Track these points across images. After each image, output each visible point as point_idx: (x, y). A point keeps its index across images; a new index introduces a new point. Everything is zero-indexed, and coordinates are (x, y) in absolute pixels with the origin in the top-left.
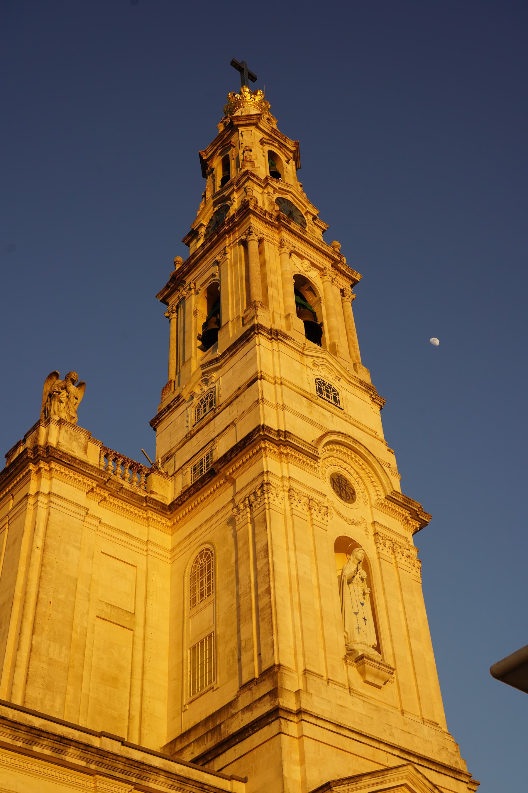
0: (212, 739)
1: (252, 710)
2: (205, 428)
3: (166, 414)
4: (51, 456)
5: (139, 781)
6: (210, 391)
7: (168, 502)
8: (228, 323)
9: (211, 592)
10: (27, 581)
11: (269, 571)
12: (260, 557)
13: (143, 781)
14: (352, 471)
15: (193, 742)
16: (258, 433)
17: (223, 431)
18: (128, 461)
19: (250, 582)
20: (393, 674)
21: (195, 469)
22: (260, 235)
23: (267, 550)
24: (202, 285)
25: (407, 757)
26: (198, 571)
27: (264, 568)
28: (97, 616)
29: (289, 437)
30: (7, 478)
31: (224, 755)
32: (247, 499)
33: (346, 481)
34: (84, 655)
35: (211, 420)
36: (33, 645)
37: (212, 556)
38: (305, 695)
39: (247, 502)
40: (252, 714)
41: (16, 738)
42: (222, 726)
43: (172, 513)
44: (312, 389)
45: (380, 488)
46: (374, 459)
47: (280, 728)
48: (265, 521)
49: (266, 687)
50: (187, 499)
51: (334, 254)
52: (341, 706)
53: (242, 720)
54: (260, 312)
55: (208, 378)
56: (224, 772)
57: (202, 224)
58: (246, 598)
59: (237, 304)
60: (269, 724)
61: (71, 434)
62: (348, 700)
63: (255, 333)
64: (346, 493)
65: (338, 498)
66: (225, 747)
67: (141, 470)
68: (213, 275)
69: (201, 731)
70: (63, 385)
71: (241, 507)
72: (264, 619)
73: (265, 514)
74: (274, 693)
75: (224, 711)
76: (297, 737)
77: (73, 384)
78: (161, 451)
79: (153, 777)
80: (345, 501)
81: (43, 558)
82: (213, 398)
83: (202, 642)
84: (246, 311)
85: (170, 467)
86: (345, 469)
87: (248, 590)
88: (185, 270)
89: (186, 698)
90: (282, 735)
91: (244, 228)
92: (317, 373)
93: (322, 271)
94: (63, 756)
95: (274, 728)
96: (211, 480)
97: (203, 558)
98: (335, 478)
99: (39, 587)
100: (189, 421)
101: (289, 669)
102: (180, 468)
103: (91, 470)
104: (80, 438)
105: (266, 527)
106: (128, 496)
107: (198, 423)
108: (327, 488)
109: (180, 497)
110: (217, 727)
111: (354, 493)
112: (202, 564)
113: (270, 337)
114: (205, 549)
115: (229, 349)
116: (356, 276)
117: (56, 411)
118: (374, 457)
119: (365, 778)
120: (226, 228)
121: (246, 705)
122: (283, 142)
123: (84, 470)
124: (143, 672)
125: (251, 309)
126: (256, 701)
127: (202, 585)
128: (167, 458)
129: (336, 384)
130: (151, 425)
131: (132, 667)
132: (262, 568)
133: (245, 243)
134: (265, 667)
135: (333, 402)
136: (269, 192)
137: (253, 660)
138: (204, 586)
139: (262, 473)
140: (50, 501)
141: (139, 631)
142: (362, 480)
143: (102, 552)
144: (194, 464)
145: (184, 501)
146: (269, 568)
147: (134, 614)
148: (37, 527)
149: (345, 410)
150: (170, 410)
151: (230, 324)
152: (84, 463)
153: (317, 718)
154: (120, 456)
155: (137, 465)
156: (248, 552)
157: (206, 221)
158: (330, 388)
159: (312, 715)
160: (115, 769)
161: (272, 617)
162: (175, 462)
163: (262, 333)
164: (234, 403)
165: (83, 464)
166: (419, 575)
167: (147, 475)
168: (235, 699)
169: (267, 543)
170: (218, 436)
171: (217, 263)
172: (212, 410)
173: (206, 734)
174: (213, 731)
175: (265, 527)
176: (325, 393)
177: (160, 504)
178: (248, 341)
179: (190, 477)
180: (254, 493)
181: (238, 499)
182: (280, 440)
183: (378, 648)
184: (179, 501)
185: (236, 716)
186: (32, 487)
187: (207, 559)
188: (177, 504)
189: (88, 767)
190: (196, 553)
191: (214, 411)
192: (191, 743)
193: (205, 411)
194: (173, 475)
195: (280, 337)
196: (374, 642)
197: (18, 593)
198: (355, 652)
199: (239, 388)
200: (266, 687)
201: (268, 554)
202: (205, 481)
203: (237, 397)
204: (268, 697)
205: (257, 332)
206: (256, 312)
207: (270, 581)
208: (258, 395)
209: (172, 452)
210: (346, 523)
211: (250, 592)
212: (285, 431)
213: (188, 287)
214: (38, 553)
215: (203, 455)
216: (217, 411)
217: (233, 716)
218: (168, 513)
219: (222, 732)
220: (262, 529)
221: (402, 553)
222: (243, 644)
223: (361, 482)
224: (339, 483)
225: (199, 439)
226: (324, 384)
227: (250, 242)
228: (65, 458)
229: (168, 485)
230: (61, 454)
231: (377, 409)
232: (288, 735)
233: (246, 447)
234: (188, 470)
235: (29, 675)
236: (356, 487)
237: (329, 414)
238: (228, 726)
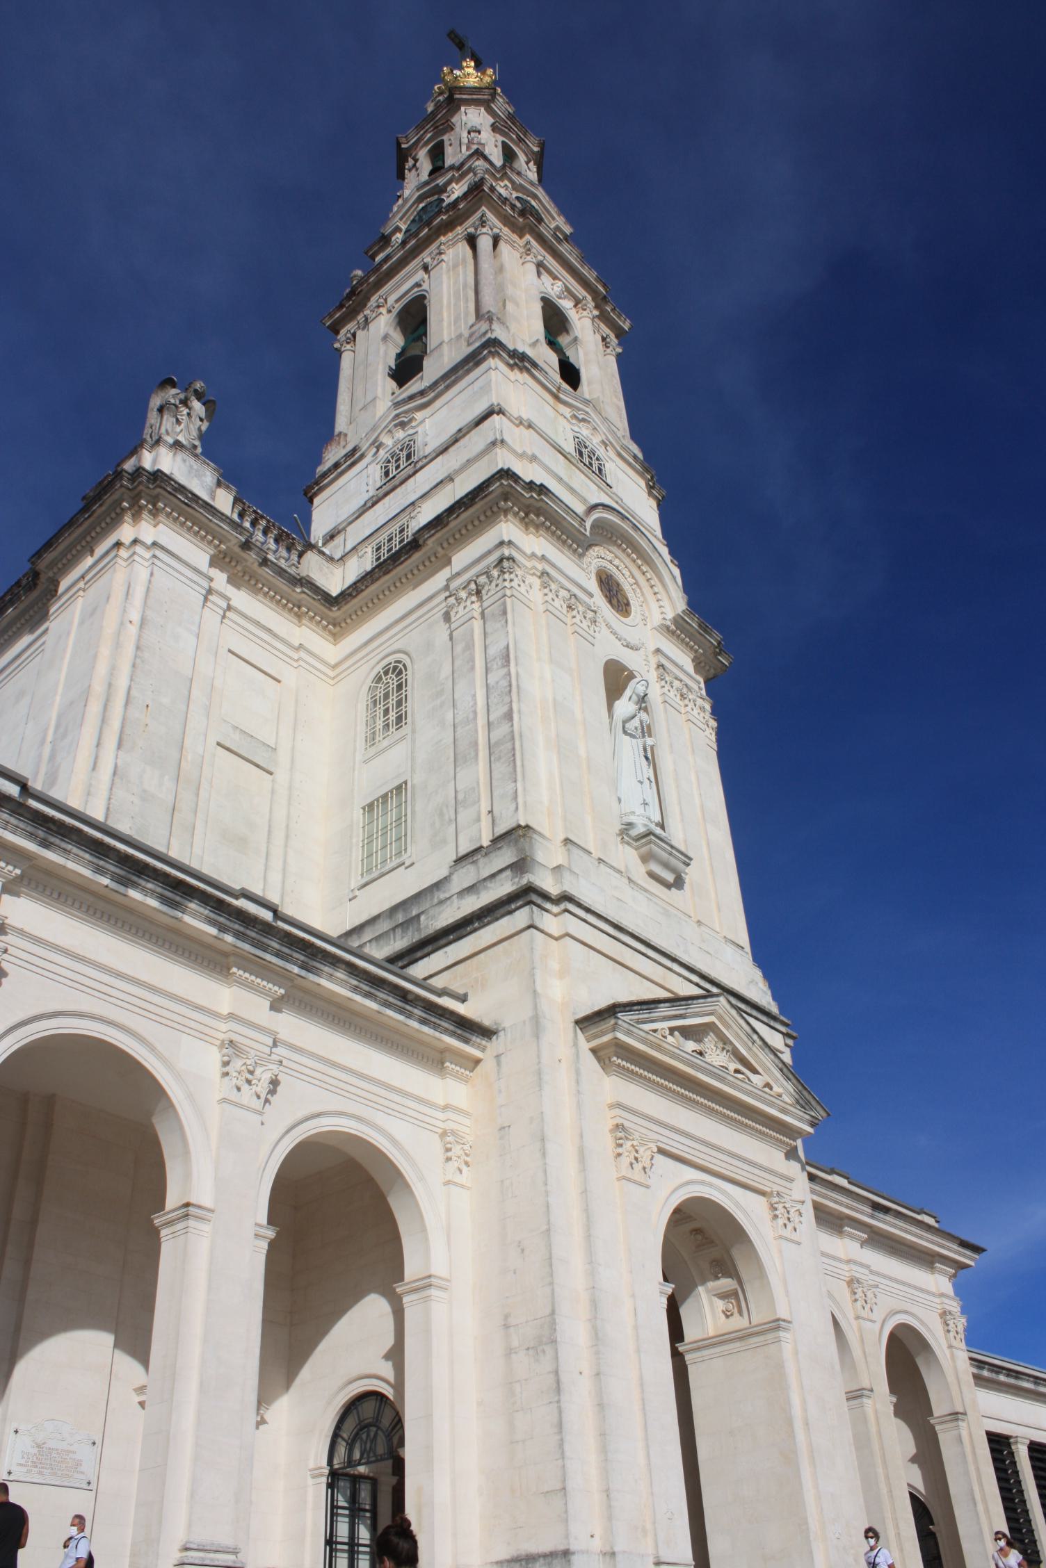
0: (402, 937)
1: (478, 893)
2: (399, 490)
3: (332, 476)
4: (161, 487)
5: (303, 973)
6: (407, 439)
7: (334, 594)
8: (441, 344)
9: (403, 723)
10: (113, 670)
11: (510, 685)
12: (495, 667)
13: (310, 974)
14: (625, 572)
15: (370, 941)
16: (499, 481)
17: (431, 489)
18: (274, 526)
19: (475, 704)
20: (688, 865)
21: (378, 549)
22: (496, 231)
23: (508, 656)
24: (397, 301)
25: (708, 986)
26: (380, 693)
27: (501, 683)
28: (219, 744)
29: (546, 495)
30: (86, 519)
31: (426, 960)
32: (473, 583)
33: (618, 585)
34: (198, 795)
35: (410, 477)
36: (119, 764)
37: (406, 670)
38: (568, 873)
39: (473, 586)
40: (478, 898)
41: (99, 870)
42: (423, 918)
43: (339, 609)
44: (570, 448)
45: (666, 602)
46: (660, 559)
47: (532, 918)
48: (505, 613)
49: (506, 856)
50: (367, 587)
51: (597, 282)
52: (619, 899)
53: (459, 908)
54: (495, 326)
55: (406, 420)
56: (432, 982)
57: (398, 229)
58: (467, 728)
59: (457, 319)
60: (510, 912)
61: (191, 467)
62: (628, 893)
63: (490, 352)
64: (618, 601)
65: (607, 604)
66: (429, 948)
67: (293, 544)
68: (418, 285)
69: (384, 926)
70: (182, 396)
71: (463, 594)
72: (500, 758)
73: (504, 604)
74: (520, 866)
75: (426, 895)
76: (556, 934)
77: (199, 399)
78: (318, 531)
79: (326, 969)
80: (617, 612)
81: (140, 637)
82: (412, 449)
83: (385, 797)
84: (472, 326)
85: (336, 547)
86: (617, 568)
87: (471, 716)
88: (371, 280)
89: (356, 881)
90: (532, 930)
91: (474, 218)
92: (576, 429)
93: (577, 302)
94: (180, 914)
95: (521, 917)
96: (410, 557)
97: (390, 675)
98: (604, 577)
99: (131, 680)
100: (371, 483)
101: (540, 834)
102: (354, 548)
103: (222, 520)
104: (205, 475)
105: (506, 621)
106: (273, 572)
107: (385, 484)
108: (593, 585)
109: (355, 583)
110: (412, 919)
111: (628, 604)
112: (388, 683)
113: (511, 362)
114: (393, 661)
115: (445, 377)
116: (624, 323)
117: (170, 430)
118: (660, 555)
119: (662, 1005)
120: (444, 218)
121: (466, 885)
122: (522, 136)
123: (210, 518)
124: (287, 837)
125: (482, 322)
126: (485, 880)
127: (386, 712)
128: (331, 537)
129: (601, 451)
130: (305, 494)
131: (270, 826)
132: (497, 683)
133: (472, 241)
134: (500, 830)
135: (597, 472)
136: (506, 185)
137: (478, 820)
138: (390, 716)
139: (502, 543)
140: (154, 556)
141: (282, 775)
142: (640, 589)
143: (230, 651)
144: (377, 541)
145: (362, 591)
146: (510, 682)
147: (275, 749)
148: (131, 591)
149: (614, 490)
150: (339, 470)
151: (445, 348)
152: (211, 506)
153: (588, 910)
154: (262, 517)
155: (288, 535)
156: (472, 660)
157: (405, 223)
158: (594, 455)
159: (579, 905)
160: (265, 948)
161: (514, 755)
162: (345, 540)
163: (501, 353)
164: (451, 450)
165: (208, 507)
166: (713, 738)
167: (300, 556)
168: (445, 878)
169: (507, 647)
170: (421, 497)
171: (426, 268)
172: (410, 464)
173: (394, 929)
174: (404, 925)
175: (503, 622)
176: (588, 459)
177: (322, 593)
178: (478, 364)
179: (371, 560)
180: (487, 573)
181: (454, 585)
182: (532, 496)
183: (662, 827)
184: (354, 589)
185: (448, 902)
186: (126, 532)
187: (396, 676)
188: (350, 595)
189: (220, 937)
190: (379, 668)
191: (415, 466)
192: (366, 943)
193: (398, 467)
194: (341, 559)
195: (526, 364)
196: (658, 818)
197: (98, 688)
198: (633, 828)
199: (460, 430)
200: (506, 856)
201: (508, 661)
202: (400, 558)
203: (456, 441)
204: (508, 873)
205: (493, 350)
206: (490, 326)
207: (511, 702)
208: (495, 434)
209: (340, 528)
210: (619, 643)
211: (475, 718)
212: (542, 485)
213: (374, 305)
214: (133, 630)
215: (395, 528)
216: (418, 466)
217: (441, 902)
218: (334, 609)
219: (422, 926)
220: (498, 625)
221: (694, 701)
222: (460, 797)
223: (638, 590)
224: (608, 584)
225: (387, 505)
226: (586, 447)
227: (480, 237)
228: (181, 493)
229: (332, 573)
230: (176, 486)
231: (654, 504)
232: (542, 931)
233: (476, 503)
234: (366, 550)
235: (111, 809)
236: (631, 596)
237: (594, 487)
238: (433, 917)
